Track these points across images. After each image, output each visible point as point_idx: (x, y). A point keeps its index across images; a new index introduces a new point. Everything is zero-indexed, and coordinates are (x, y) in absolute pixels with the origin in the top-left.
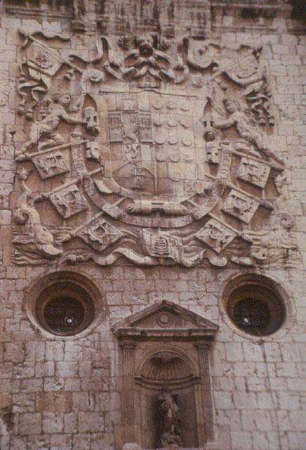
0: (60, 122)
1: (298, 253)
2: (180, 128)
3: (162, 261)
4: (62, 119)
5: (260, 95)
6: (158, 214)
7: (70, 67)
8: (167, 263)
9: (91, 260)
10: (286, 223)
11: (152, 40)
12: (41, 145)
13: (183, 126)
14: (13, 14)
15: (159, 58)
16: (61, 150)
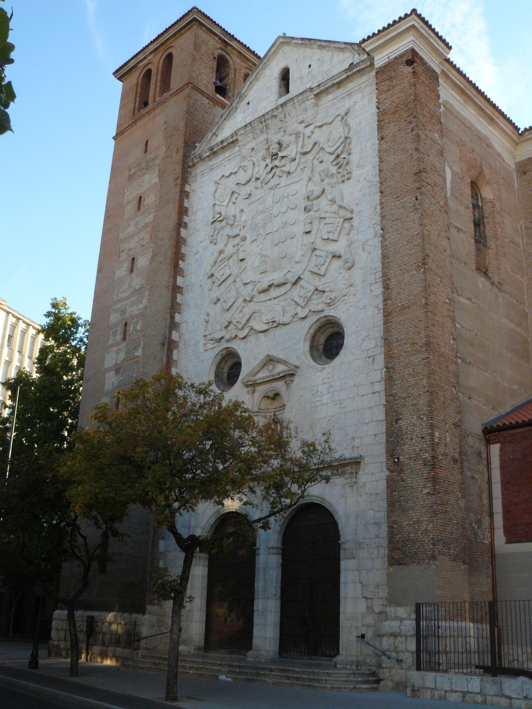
0: (228, 239)
1: (353, 288)
2: (290, 211)
3: (271, 324)
4: (229, 237)
5: (342, 156)
6: (273, 287)
7: (236, 193)
8: (275, 325)
9: (236, 336)
10: (347, 265)
11: (278, 145)
12: (219, 260)
13: (291, 209)
14: (212, 169)
15: (283, 157)
16: (228, 259)
